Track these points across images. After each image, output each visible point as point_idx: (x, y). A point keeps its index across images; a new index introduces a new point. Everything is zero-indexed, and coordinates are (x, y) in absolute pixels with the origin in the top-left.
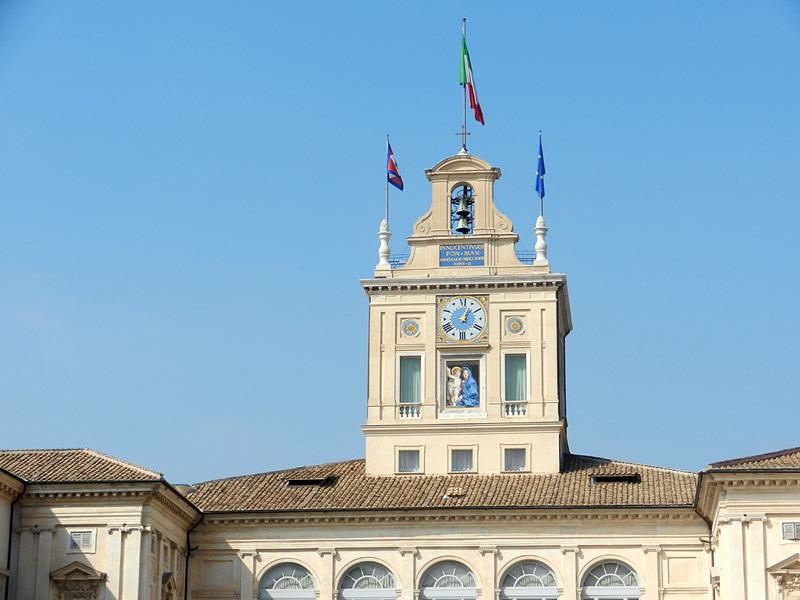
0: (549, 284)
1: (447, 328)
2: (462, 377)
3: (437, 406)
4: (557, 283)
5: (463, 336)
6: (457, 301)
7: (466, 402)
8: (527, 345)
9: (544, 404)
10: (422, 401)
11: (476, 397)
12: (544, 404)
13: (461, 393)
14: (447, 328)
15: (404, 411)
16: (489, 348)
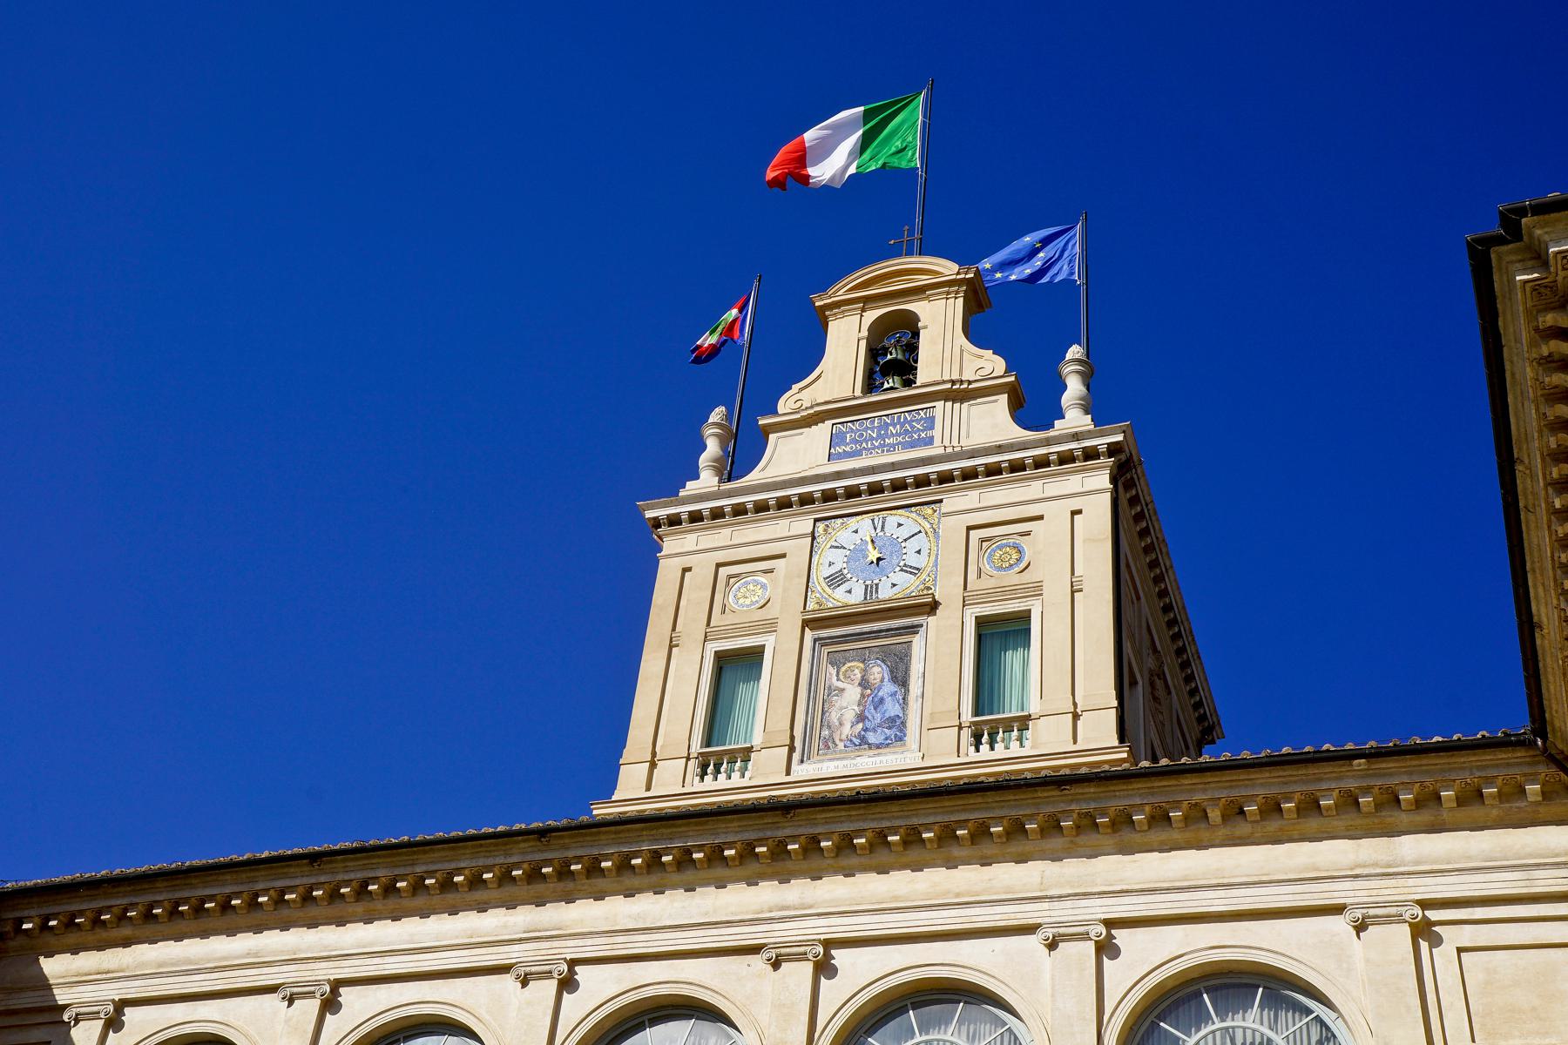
0: (1090, 454)
1: (836, 580)
2: (864, 684)
3: (792, 749)
4: (1113, 450)
5: (871, 589)
6: (864, 523)
7: (872, 738)
8: (1036, 590)
9: (1076, 717)
10: (757, 740)
11: (897, 726)
12: (1076, 717)
13: (861, 718)
14: (836, 580)
15: (711, 769)
16: (933, 607)
